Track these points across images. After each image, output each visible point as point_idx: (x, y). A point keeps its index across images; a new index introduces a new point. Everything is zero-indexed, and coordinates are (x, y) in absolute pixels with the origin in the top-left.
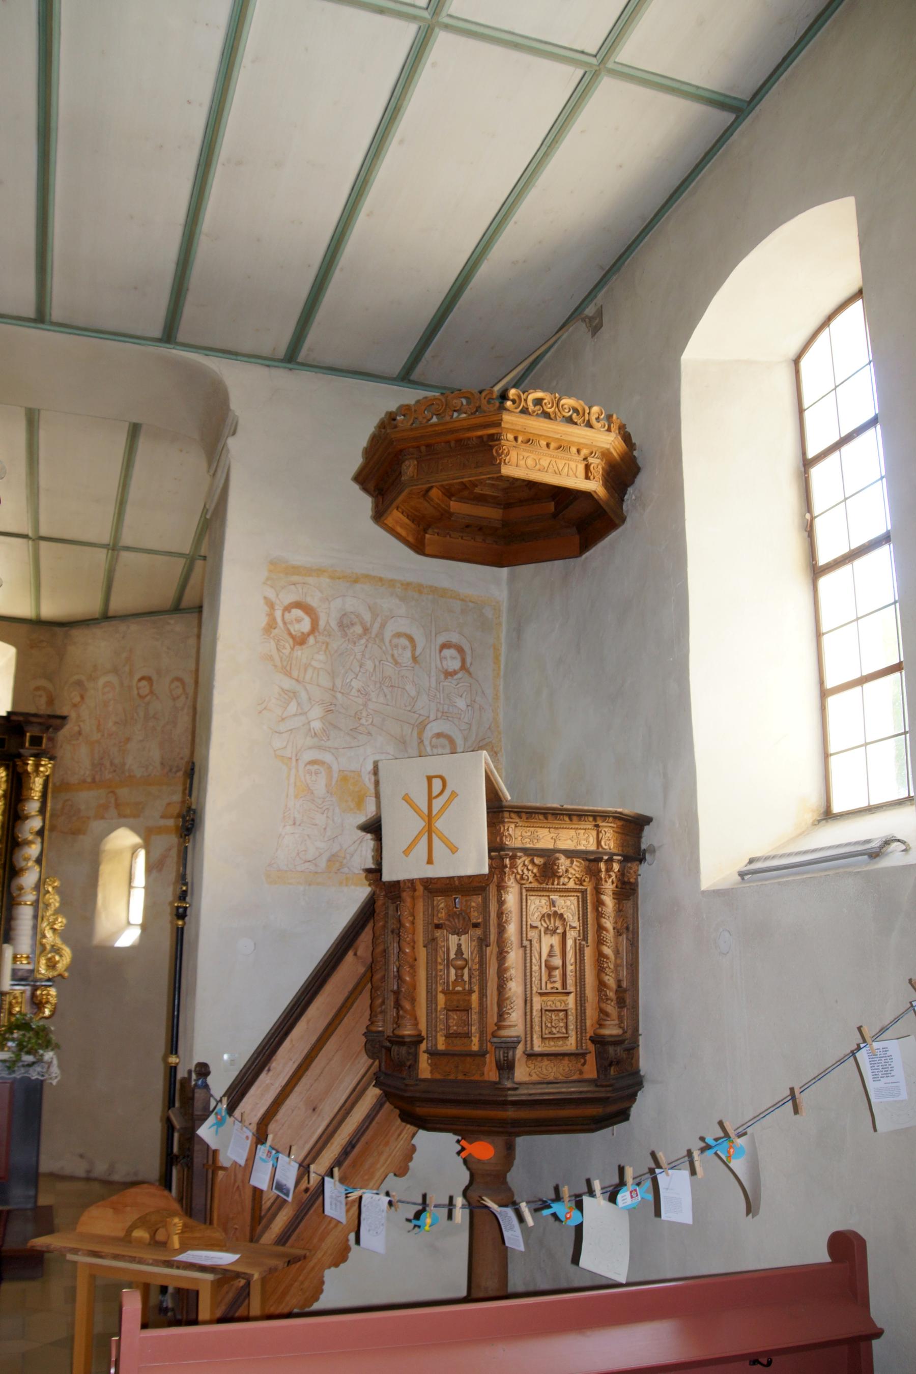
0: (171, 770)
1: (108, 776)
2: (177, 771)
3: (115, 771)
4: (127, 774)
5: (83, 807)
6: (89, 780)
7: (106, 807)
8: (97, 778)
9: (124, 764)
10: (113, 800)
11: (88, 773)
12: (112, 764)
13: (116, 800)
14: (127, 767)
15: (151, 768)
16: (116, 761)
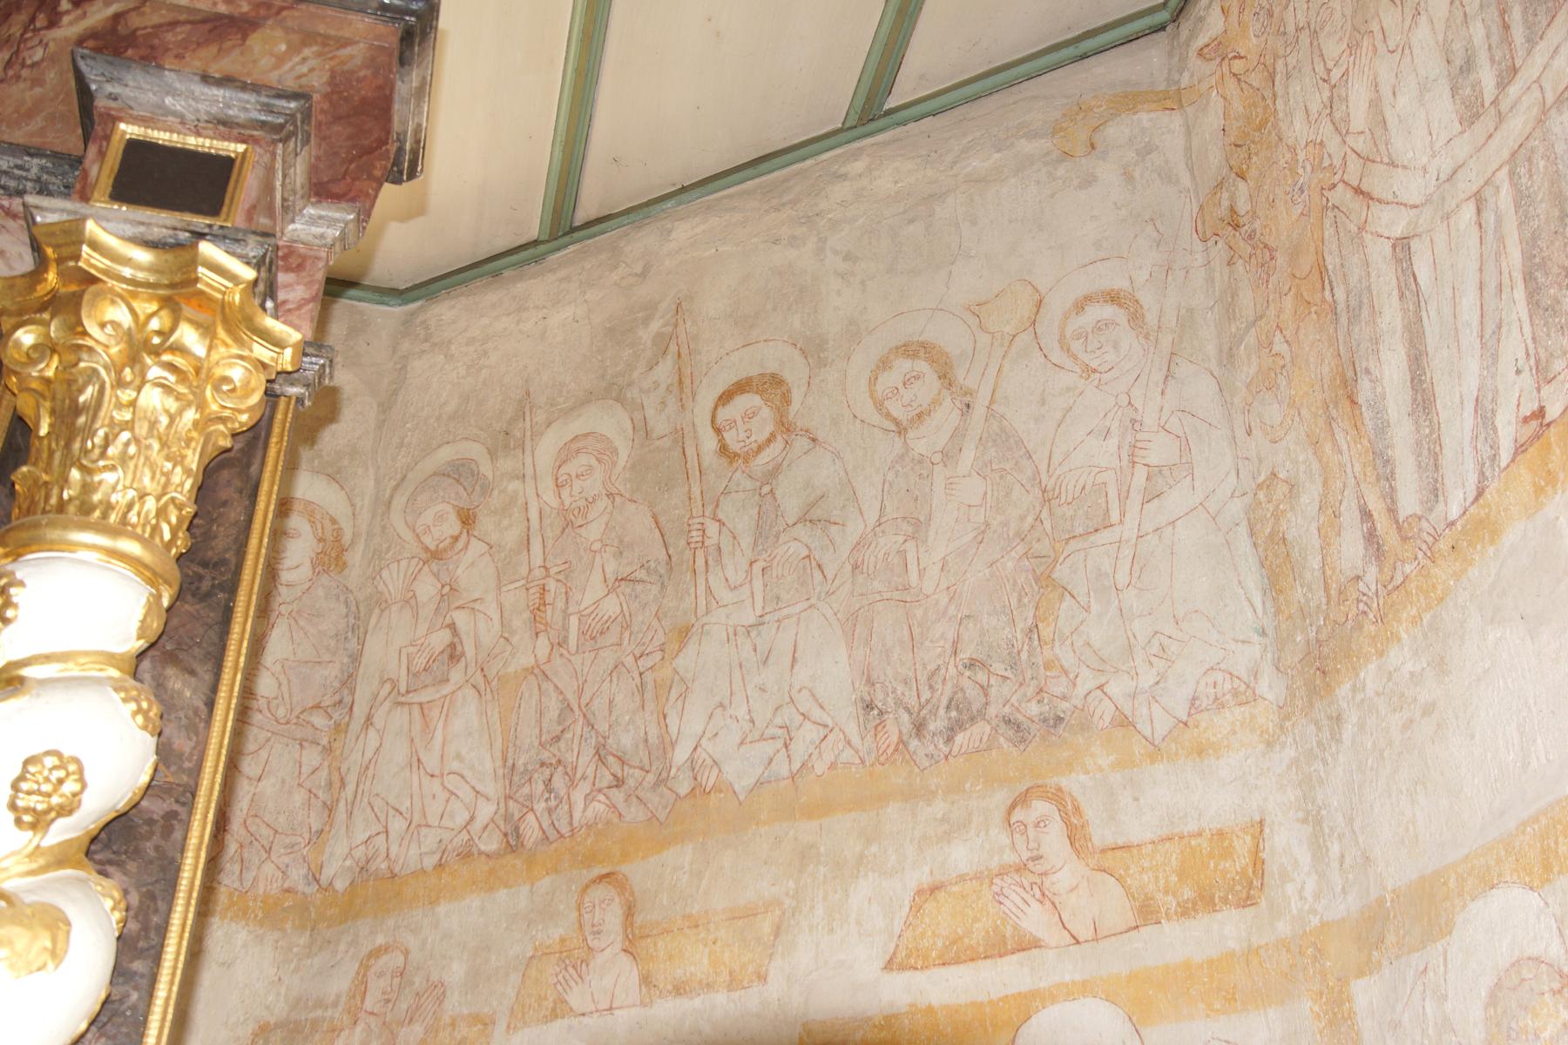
0: (919, 728)
1: (585, 807)
2: (950, 734)
3: (619, 782)
4: (683, 789)
5: (456, 972)
6: (491, 844)
7: (575, 958)
8: (531, 830)
9: (667, 744)
10: (612, 918)
11: (486, 811)
12: (600, 755)
13: (630, 912)
14: (681, 755)
15: (809, 733)
16: (626, 740)
